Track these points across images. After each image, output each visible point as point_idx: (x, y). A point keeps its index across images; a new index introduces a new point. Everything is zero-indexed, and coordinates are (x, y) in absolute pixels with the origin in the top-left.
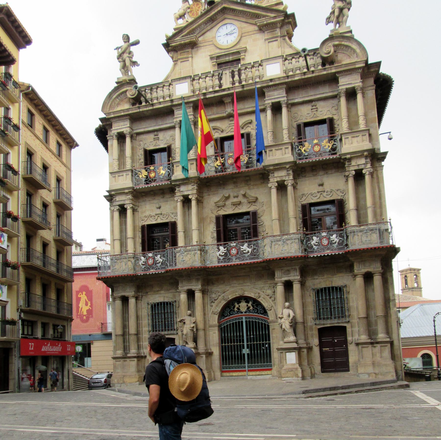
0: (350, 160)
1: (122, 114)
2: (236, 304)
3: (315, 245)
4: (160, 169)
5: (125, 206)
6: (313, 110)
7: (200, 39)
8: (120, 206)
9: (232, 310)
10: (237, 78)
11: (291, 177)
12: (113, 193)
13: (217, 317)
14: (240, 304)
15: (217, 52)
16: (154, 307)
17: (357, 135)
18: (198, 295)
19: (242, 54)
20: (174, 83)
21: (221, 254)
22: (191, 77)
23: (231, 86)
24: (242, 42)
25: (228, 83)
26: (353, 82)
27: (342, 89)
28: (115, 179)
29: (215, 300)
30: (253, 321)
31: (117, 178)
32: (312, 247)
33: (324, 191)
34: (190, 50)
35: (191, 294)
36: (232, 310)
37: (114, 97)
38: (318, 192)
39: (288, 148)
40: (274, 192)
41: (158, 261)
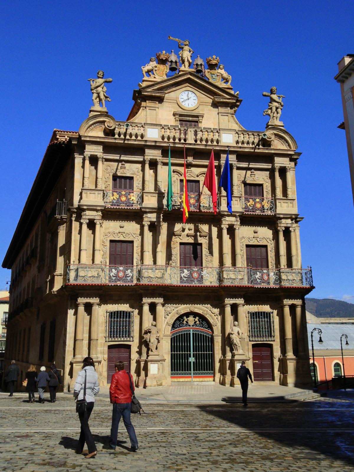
0: (281, 219)
1: (98, 140)
2: (185, 317)
3: (258, 279)
4: (131, 196)
5: (95, 221)
6: (252, 175)
7: (166, 95)
8: (89, 219)
9: (181, 323)
10: (199, 137)
11: (239, 223)
12: (85, 207)
13: (170, 328)
14: (188, 318)
15: (180, 111)
16: (112, 315)
17: (287, 202)
18: (160, 309)
19: (200, 118)
20: (146, 126)
21: (185, 276)
22: (161, 125)
23: (194, 142)
24: (199, 108)
25: (192, 139)
26: (285, 163)
27: (277, 166)
28: (87, 195)
29: (170, 313)
30: (198, 334)
31: (89, 194)
32: (257, 280)
33: (258, 238)
34: (157, 102)
35: (153, 308)
36: (181, 323)
37: (91, 123)
38: (254, 237)
39: (237, 200)
40: (225, 232)
41: (128, 274)
